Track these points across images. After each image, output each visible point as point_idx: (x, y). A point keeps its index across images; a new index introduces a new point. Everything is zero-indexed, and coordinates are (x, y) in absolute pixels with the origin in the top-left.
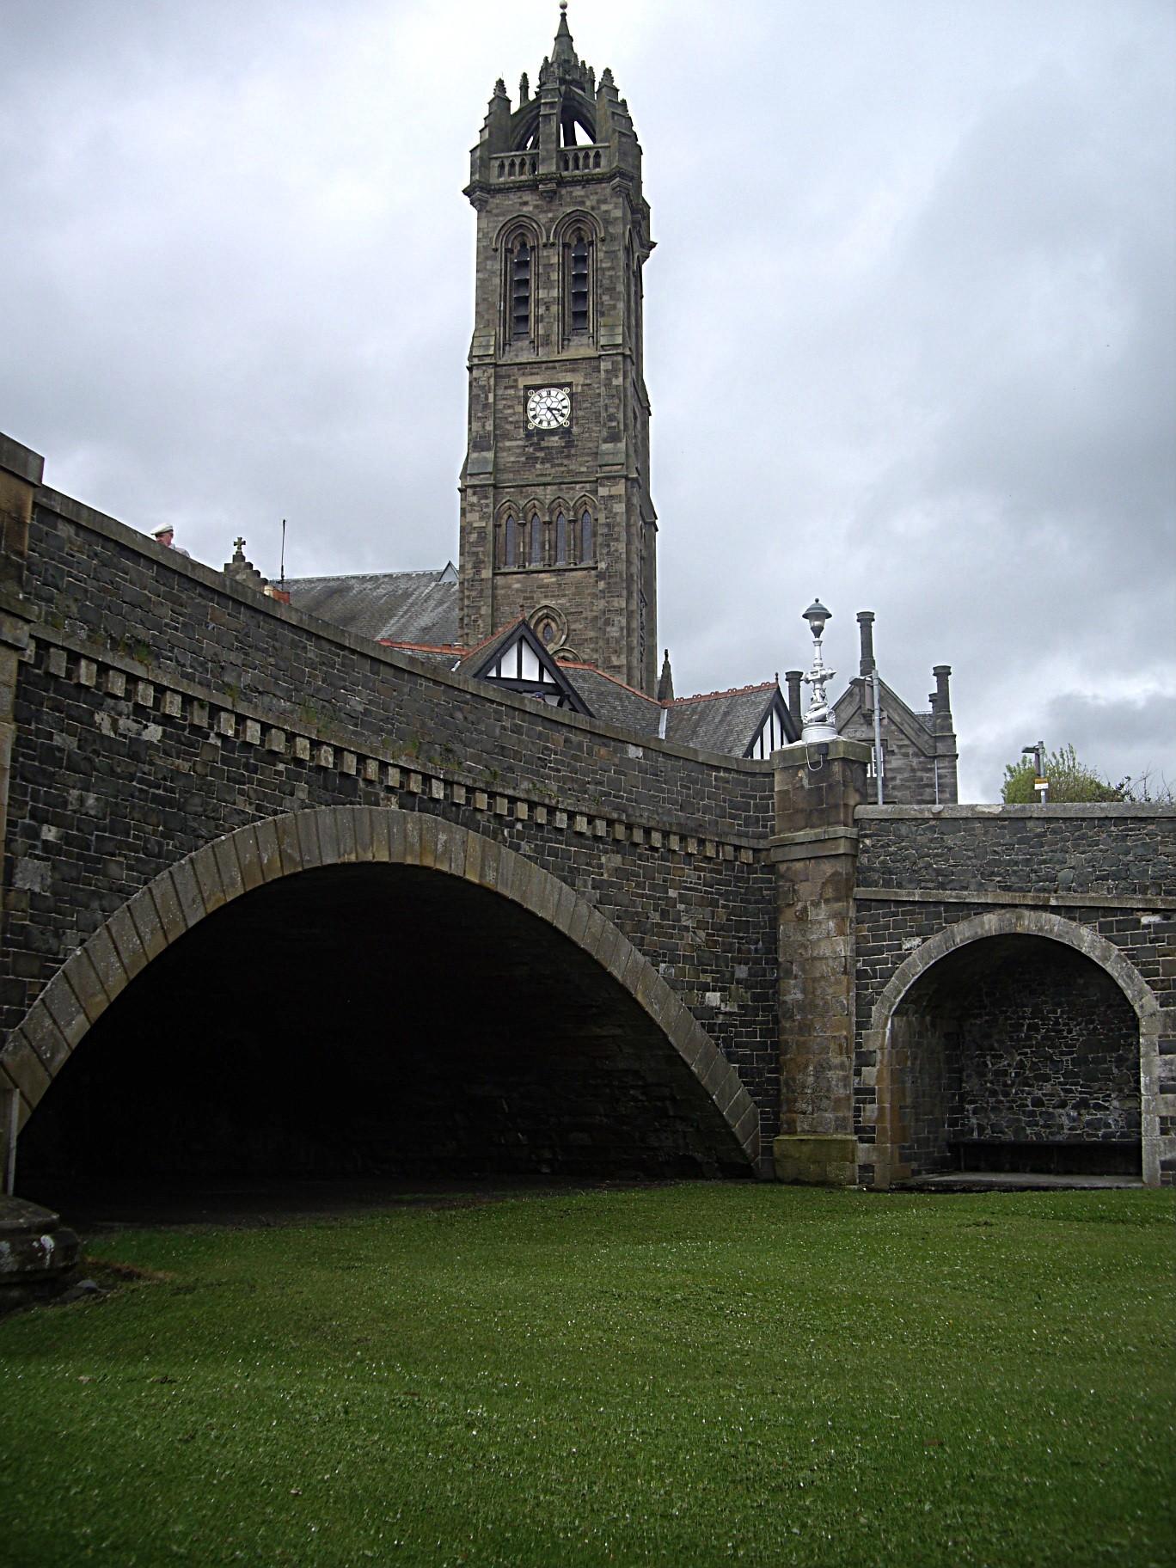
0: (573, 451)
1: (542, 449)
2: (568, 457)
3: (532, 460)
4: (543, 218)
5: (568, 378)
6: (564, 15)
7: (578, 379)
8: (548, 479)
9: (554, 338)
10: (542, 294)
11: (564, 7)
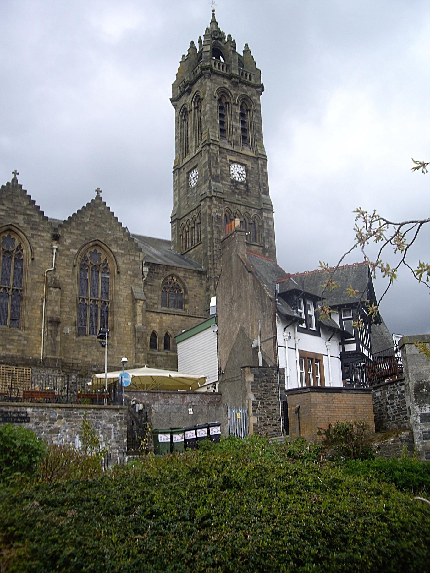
0: (249, 194)
1: (237, 189)
2: (248, 195)
3: (234, 193)
4: (233, 92)
5: (245, 162)
6: (213, 14)
7: (249, 164)
8: (241, 203)
9: (239, 143)
10: (234, 123)
11: (213, 11)
